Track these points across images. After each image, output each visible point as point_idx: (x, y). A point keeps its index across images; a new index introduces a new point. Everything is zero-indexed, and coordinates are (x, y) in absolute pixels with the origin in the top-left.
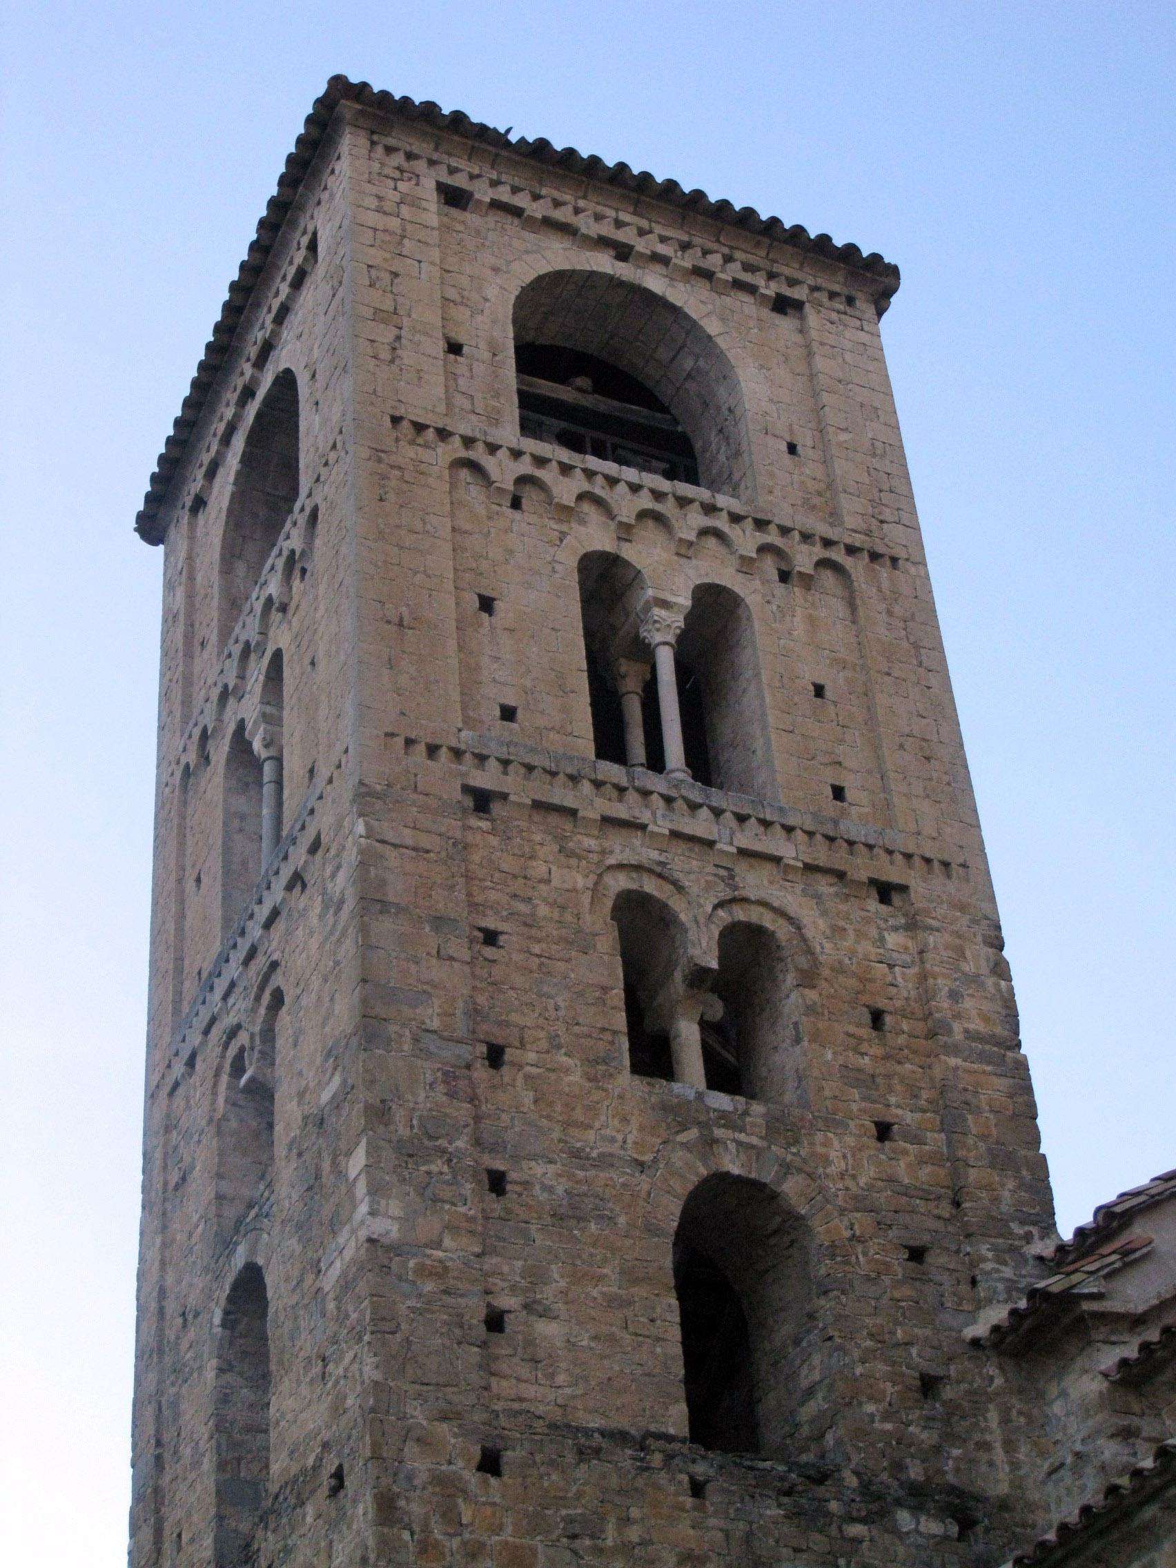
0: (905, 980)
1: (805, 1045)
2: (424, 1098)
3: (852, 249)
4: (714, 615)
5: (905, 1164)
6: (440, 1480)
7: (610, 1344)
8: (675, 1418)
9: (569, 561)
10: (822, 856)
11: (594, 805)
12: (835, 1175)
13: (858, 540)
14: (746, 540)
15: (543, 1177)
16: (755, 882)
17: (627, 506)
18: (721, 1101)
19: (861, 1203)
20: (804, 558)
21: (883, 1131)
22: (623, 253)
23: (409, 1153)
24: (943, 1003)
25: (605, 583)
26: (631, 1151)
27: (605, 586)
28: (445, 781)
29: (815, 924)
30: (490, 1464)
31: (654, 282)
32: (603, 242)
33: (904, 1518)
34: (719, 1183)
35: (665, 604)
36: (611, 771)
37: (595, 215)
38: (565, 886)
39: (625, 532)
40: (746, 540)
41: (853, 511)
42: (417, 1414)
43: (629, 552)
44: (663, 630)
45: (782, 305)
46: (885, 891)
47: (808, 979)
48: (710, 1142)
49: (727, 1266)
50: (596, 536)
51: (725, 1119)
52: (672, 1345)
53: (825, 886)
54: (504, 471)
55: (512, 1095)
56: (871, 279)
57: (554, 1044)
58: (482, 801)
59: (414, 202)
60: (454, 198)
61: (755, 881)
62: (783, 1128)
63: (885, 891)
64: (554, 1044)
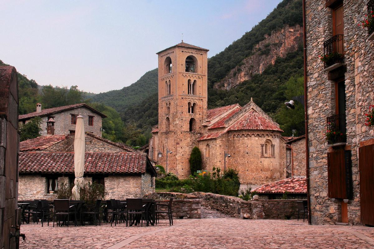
0: (202, 105)
1: (197, 109)
2: (179, 116)
4: (195, 81)
5: (201, 116)
6: (180, 134)
7: (186, 127)
8: (189, 130)
10: (198, 98)
11: (187, 97)
12: (197, 117)
13: (203, 74)
14: (197, 76)
15: (184, 119)
16: (195, 100)
17: (191, 75)
18: (192, 114)
19: (198, 118)
20: (200, 77)
21: (200, 114)
22: (192, 53)
23: (179, 119)
24: (204, 106)
25: (189, 81)
26: (187, 117)
27: (189, 81)
28: (180, 97)
29: (198, 102)
30: (181, 133)
31: (194, 55)
33: (198, 134)
34: (192, 118)
36: (189, 95)
37: (190, 51)
38: (186, 103)
40: (197, 76)
41: (203, 72)
44: (192, 83)
45: (201, 54)
46: (202, 100)
47: (197, 106)
48: (191, 116)
49: (192, 121)
50: (189, 78)
51: (192, 115)
52: (189, 127)
53: (199, 100)
54: (184, 75)
55: (183, 115)
56: (207, 51)
58: (182, 98)
59: (180, 53)
60: (182, 51)
61: (195, 100)
62: (195, 115)
63: (202, 100)
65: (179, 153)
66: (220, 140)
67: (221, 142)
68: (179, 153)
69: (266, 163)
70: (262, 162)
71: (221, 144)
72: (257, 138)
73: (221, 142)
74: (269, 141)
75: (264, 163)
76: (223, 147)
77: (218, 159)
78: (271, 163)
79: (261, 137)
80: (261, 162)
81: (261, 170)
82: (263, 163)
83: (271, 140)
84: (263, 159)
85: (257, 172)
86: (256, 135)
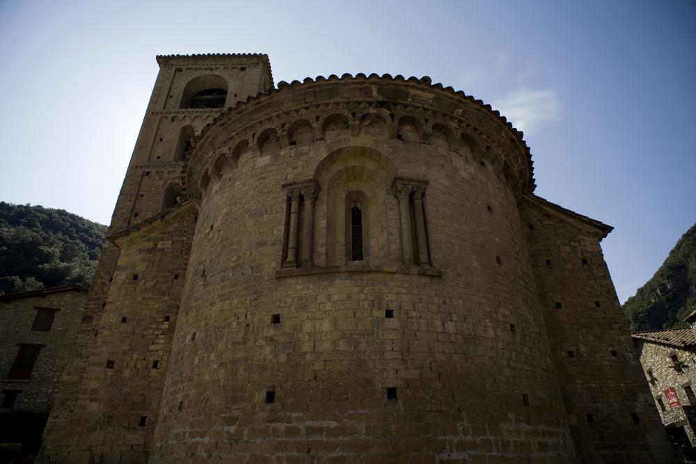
3: (255, 54)
9: (180, 128)
28: (140, 172)
32: (206, 69)
35: (197, 131)
39: (193, 121)
42: (102, 274)
43: (193, 124)
45: (243, 69)
50: (187, 122)
57: (148, 210)
64: (148, 210)
65: (81, 356)
66: (141, 251)
67: (143, 260)
68: (81, 356)
69: (326, 326)
70: (287, 324)
71: (141, 268)
72: (264, 160)
73: (143, 260)
74: (370, 165)
75: (308, 327)
76: (150, 284)
77: (105, 348)
78: (393, 323)
79: (293, 143)
80: (276, 319)
81: (270, 397)
82: (298, 329)
83: (384, 149)
84: (299, 288)
85: (231, 421)
86: (253, 143)
